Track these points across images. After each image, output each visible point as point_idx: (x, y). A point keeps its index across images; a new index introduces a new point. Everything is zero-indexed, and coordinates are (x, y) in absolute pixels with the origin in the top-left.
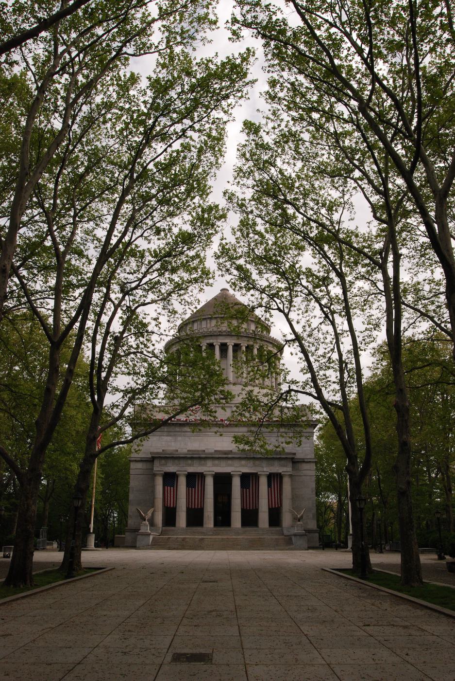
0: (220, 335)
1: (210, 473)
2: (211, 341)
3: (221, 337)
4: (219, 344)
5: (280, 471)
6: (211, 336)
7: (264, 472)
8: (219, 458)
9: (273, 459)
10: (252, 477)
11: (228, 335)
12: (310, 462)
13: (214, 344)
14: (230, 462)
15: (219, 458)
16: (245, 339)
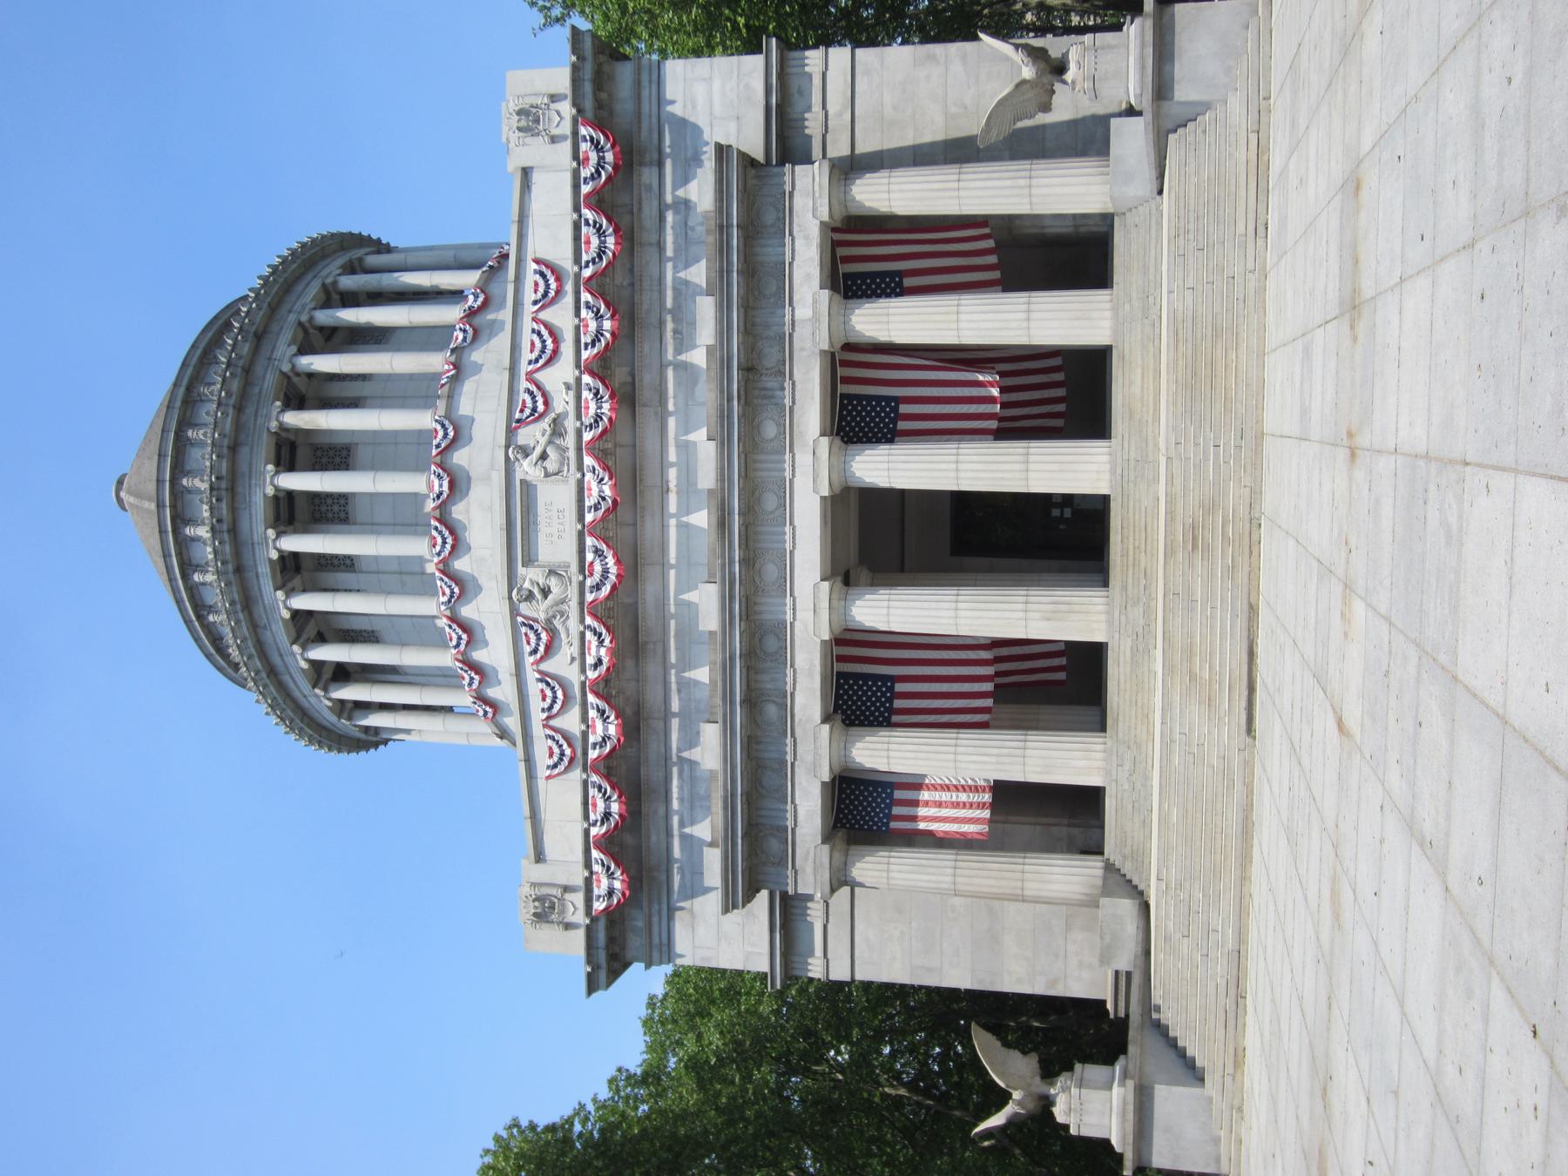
0: (234, 531)
1: (824, 604)
2: (264, 570)
3: (244, 525)
4: (271, 533)
5: (814, 231)
6: (239, 570)
7: (816, 317)
8: (750, 561)
9: (751, 271)
10: (846, 380)
11: (232, 490)
12: (782, 75)
13: (274, 555)
14: (770, 502)
15: (749, 561)
16: (250, 410)
